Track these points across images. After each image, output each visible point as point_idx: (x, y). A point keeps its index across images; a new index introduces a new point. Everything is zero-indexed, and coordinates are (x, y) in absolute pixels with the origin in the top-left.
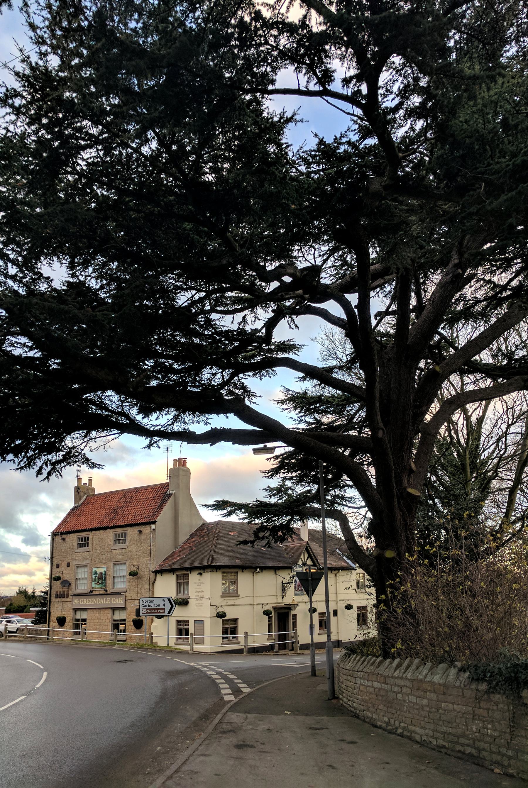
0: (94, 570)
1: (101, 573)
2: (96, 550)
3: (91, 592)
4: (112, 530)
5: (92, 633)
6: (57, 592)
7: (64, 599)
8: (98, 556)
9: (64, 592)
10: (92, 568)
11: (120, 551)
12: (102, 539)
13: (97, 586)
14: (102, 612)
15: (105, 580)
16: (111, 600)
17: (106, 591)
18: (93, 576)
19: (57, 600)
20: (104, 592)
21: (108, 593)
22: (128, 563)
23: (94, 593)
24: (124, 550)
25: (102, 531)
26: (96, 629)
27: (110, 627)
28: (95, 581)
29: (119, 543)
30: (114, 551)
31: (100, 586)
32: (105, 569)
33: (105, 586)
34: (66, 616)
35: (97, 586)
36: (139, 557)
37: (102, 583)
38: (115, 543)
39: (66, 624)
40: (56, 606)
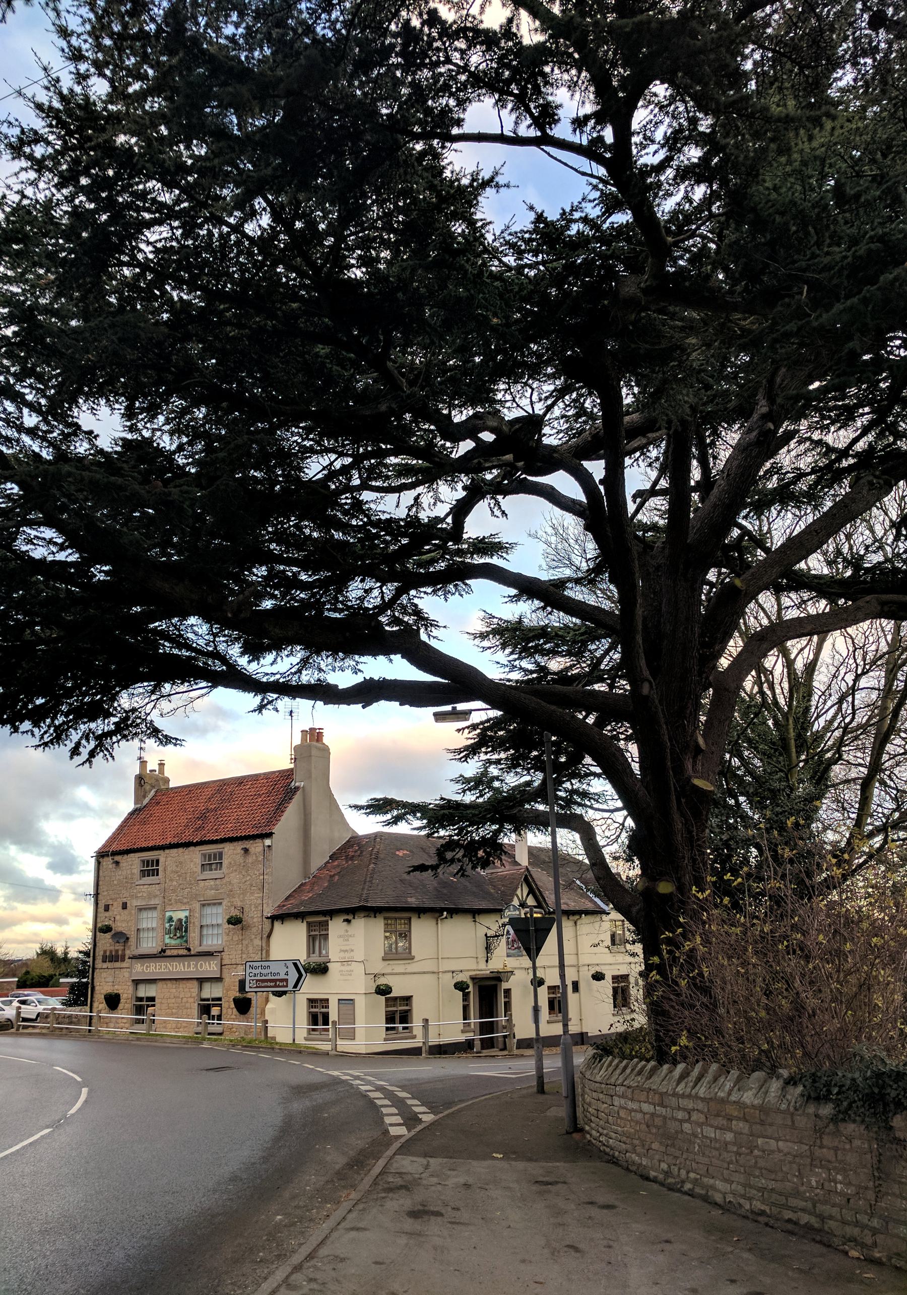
0: (168, 914)
1: (180, 920)
2: (171, 880)
3: (163, 951)
5: (165, 1021)
6: (105, 952)
7: (118, 965)
8: (174, 891)
9: (117, 951)
11: (212, 883)
12: (181, 863)
13: (173, 942)
14: (182, 985)
15: (186, 931)
17: (189, 950)
18: (167, 925)
19: (105, 965)
20: (185, 952)
22: (225, 902)
23: (168, 953)
24: (218, 882)
25: (181, 850)
26: (172, 1015)
27: (195, 1011)
28: (169, 932)
30: (202, 884)
31: (178, 941)
32: (187, 913)
33: (186, 941)
34: (120, 992)
35: (173, 942)
36: (244, 893)
37: (181, 937)
39: (121, 1006)
40: (104, 975)
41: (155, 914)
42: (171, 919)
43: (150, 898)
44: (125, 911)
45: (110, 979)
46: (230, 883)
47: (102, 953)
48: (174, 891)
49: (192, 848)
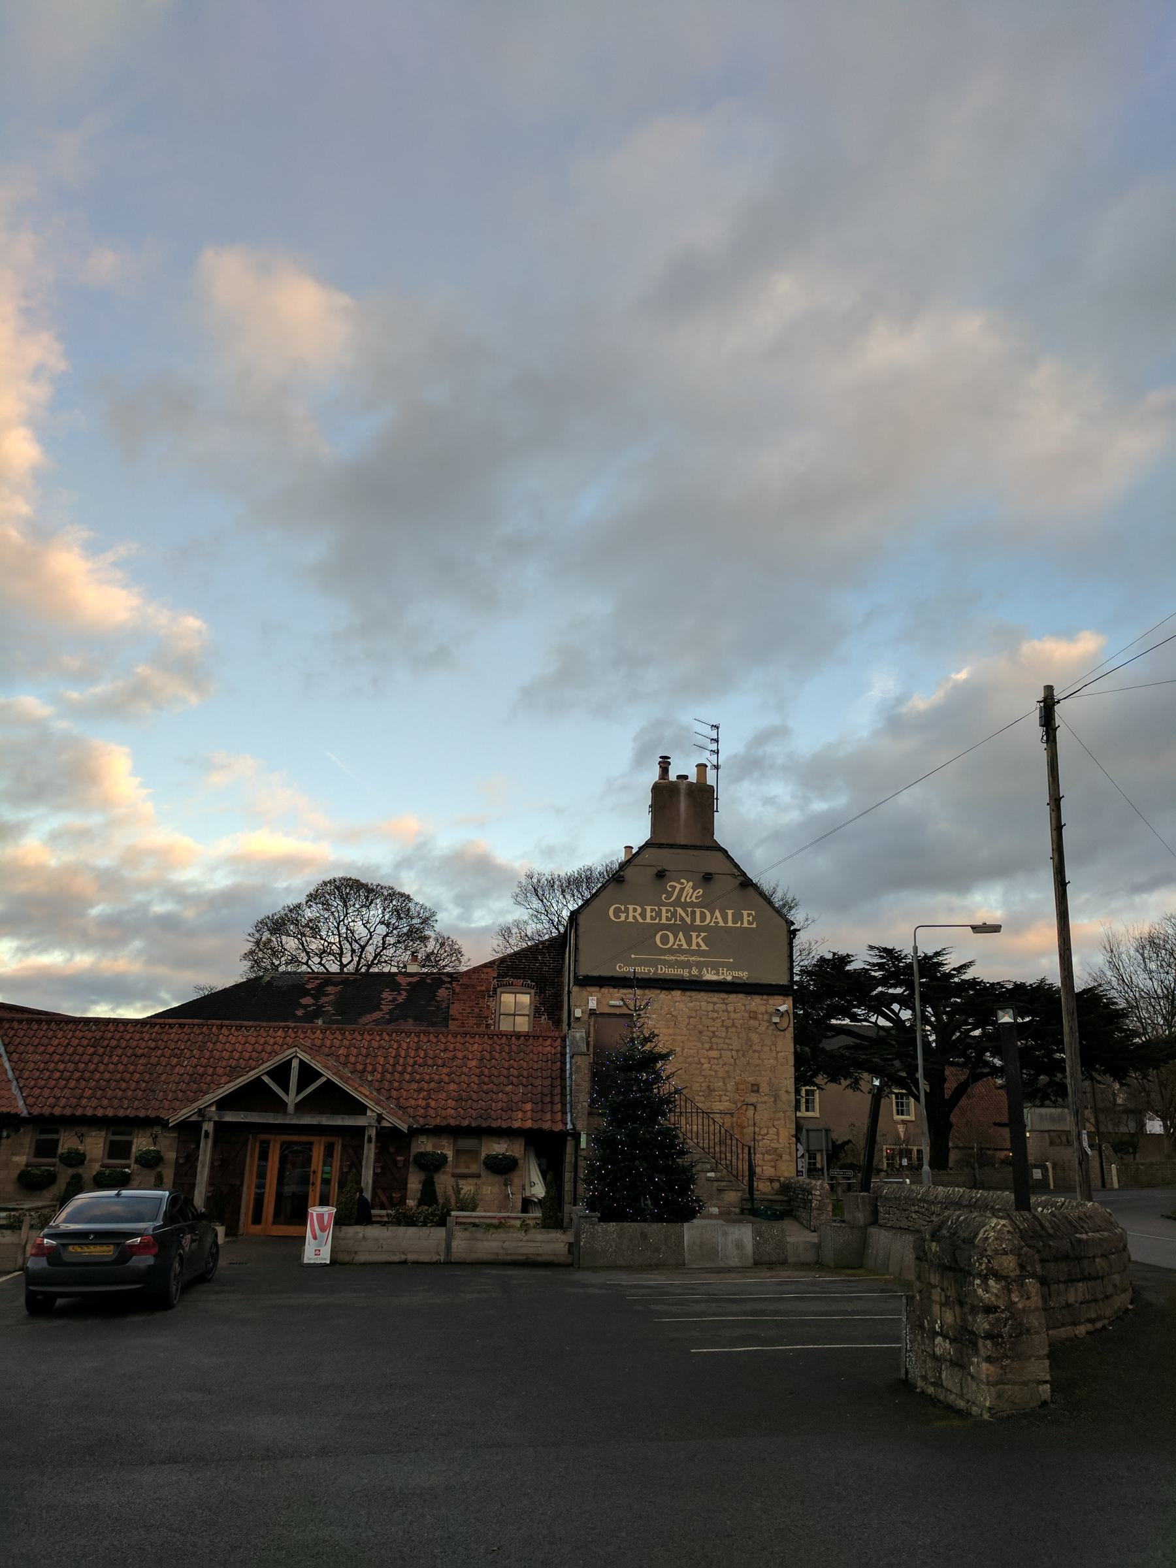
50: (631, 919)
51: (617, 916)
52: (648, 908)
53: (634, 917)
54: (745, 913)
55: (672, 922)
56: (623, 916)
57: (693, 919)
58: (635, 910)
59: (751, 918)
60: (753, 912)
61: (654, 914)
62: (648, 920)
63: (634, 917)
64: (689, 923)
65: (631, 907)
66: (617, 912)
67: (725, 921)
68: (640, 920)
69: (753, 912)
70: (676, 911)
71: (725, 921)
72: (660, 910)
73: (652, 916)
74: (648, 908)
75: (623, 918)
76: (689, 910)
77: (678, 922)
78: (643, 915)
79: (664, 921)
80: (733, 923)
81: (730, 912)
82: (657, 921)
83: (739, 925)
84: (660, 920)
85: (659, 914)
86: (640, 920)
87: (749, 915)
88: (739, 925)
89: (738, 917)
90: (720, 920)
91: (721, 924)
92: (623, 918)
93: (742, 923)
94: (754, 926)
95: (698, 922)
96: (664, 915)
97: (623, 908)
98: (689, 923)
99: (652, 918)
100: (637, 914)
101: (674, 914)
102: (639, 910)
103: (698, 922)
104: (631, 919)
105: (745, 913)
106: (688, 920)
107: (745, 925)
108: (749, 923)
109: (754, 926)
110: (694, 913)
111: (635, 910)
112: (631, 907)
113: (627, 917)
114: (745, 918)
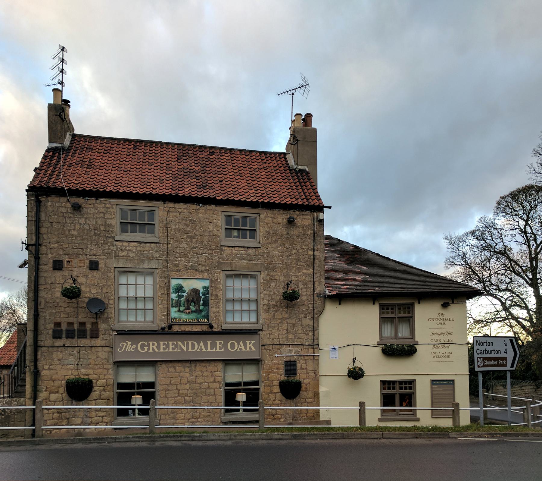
1: (196, 291)
3: (170, 327)
4: (220, 208)
5: (174, 411)
6: (58, 325)
8: (184, 255)
9: (82, 324)
10: (168, 279)
11: (243, 251)
13: (185, 317)
14: (199, 368)
15: (206, 303)
16: (225, 346)
17: (211, 327)
18: (174, 296)
19: (58, 343)
20: (205, 328)
21: (215, 330)
22: (262, 276)
23: (175, 329)
24: (251, 251)
27: (222, 398)
28: (178, 304)
29: (244, 237)
30: (228, 251)
31: (193, 316)
32: (207, 283)
33: (207, 317)
34: (91, 377)
35: (185, 317)
36: (288, 267)
37: (198, 311)
38: (228, 235)
39: (94, 395)
40: (57, 355)
41: (149, 280)
42: (179, 289)
43: (142, 260)
44: (95, 273)
45: (72, 360)
46: (269, 255)
47: (52, 326)
48: (184, 255)
49: (210, 207)
50: (151, 350)
51: (142, 348)
52: (161, 343)
53: (153, 349)
54: (218, 342)
55: (176, 351)
56: (146, 348)
57: (188, 348)
58: (153, 345)
59: (221, 346)
60: (222, 342)
61: (165, 346)
62: (162, 350)
63: (153, 349)
64: (186, 351)
65: (151, 343)
66: (142, 346)
67: (206, 348)
68: (157, 350)
69: (222, 342)
70: (177, 344)
71: (206, 348)
72: (168, 344)
73: (163, 347)
74: (161, 343)
75: (146, 350)
76: (186, 342)
77: (179, 351)
78: (158, 347)
79: (171, 350)
80: (211, 349)
81: (209, 343)
82: (167, 351)
83: (214, 350)
84: (169, 350)
85: (168, 346)
86: (157, 350)
87: (220, 344)
88: (214, 350)
89: (213, 346)
90: (203, 348)
91: (204, 350)
92: (146, 350)
93: (216, 349)
94: (223, 350)
95: (190, 350)
96: (171, 346)
97: (146, 343)
98: (186, 351)
99: (164, 349)
100: (154, 347)
101: (177, 346)
102: (156, 344)
103: (190, 350)
104: (151, 350)
105: (218, 342)
106: (185, 349)
107: (218, 350)
108: (220, 348)
109: (223, 350)
110: (188, 344)
111: (153, 345)
112: (151, 343)
113: (149, 349)
114: (218, 346)
